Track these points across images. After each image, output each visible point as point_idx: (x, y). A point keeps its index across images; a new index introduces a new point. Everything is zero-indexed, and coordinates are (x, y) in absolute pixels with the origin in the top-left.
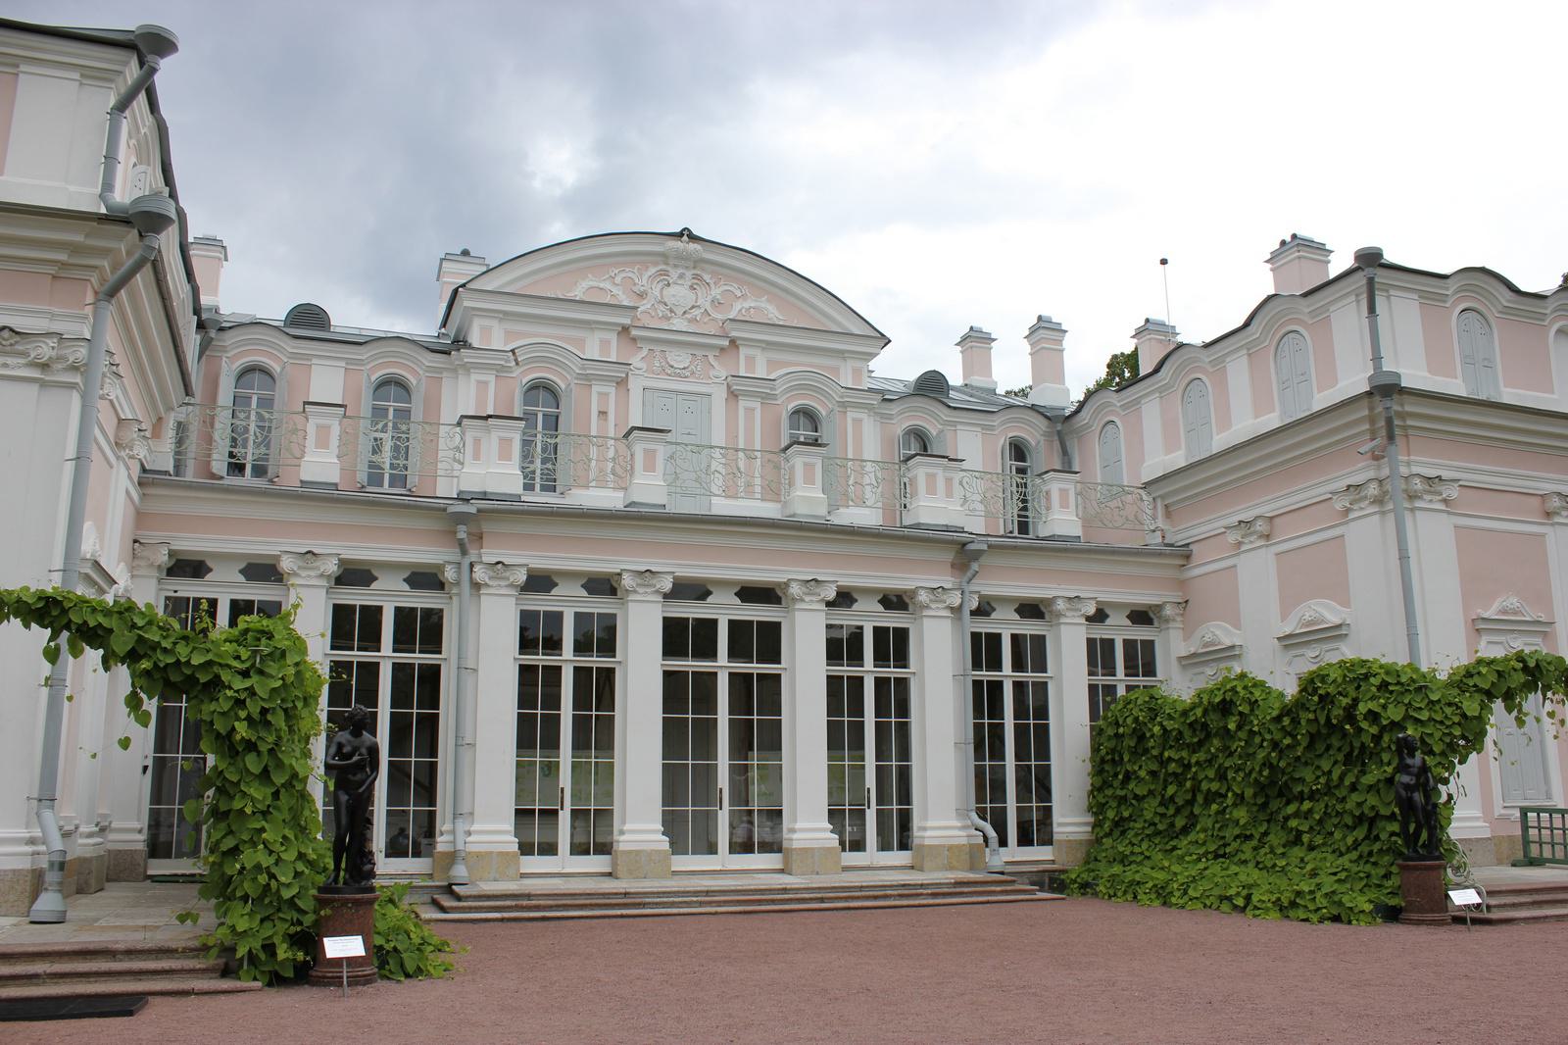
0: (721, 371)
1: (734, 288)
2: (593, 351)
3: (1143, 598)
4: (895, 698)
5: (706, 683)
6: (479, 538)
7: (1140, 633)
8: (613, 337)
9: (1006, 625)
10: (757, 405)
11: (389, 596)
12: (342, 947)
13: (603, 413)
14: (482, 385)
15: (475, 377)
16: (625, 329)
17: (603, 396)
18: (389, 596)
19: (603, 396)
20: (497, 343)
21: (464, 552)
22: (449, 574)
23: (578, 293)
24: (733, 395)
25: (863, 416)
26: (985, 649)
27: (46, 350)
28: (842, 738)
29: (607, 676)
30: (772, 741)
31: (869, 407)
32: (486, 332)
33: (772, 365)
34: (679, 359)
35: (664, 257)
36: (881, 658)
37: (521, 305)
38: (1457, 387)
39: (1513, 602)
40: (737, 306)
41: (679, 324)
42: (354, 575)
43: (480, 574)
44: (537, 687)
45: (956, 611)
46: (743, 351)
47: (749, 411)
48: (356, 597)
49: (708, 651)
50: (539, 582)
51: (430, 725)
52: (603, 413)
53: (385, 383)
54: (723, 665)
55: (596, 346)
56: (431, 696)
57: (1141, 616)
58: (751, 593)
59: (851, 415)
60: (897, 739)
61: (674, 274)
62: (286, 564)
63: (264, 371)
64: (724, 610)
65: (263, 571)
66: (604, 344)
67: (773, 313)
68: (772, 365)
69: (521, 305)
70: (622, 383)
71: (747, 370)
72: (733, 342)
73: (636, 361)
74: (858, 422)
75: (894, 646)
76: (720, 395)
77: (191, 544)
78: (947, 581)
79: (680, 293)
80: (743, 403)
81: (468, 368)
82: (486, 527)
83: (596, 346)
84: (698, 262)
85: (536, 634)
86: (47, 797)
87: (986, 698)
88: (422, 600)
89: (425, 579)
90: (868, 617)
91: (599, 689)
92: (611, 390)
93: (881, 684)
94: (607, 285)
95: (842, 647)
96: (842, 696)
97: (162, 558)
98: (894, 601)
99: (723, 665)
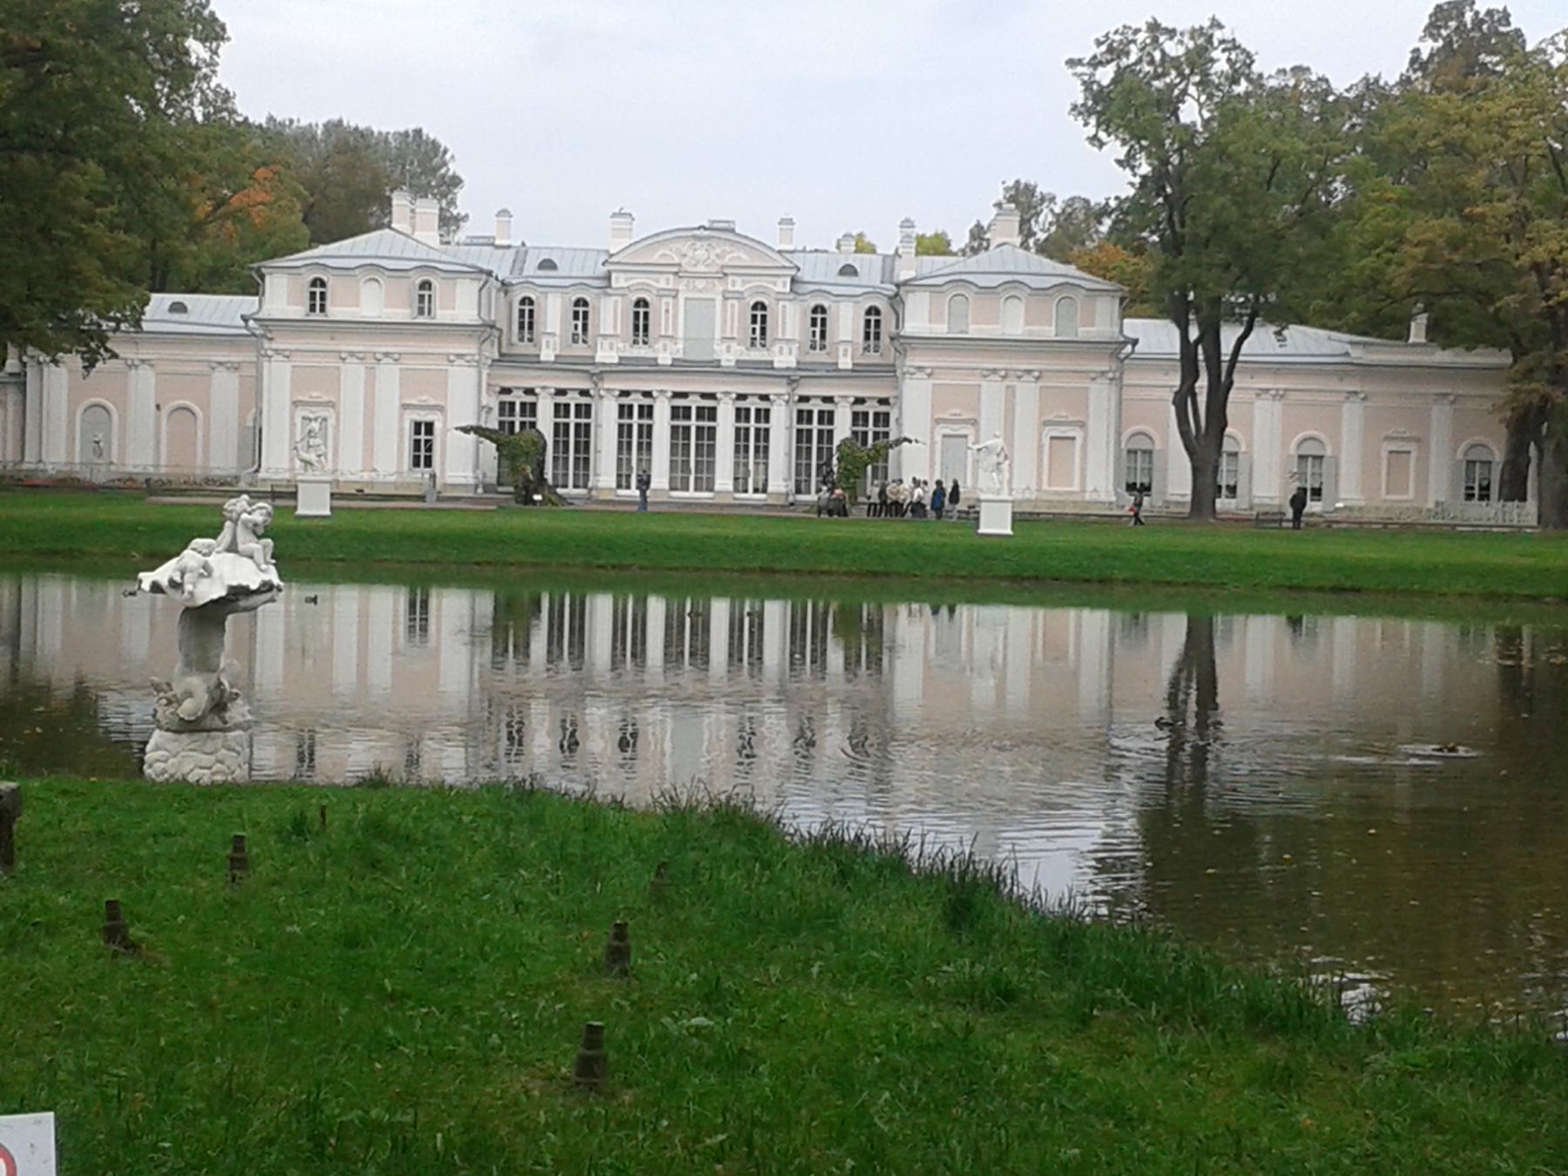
0: (720, 288)
1: (727, 248)
2: (662, 285)
3: (883, 395)
4: (763, 435)
5: (687, 429)
6: (602, 379)
7: (883, 409)
8: (671, 277)
9: (816, 407)
10: (735, 302)
11: (573, 399)
12: (537, 497)
13: (667, 311)
14: (616, 302)
15: (614, 298)
16: (676, 273)
17: (667, 304)
18: (573, 399)
19: (667, 304)
20: (623, 284)
21: (596, 385)
22: (592, 392)
23: (655, 259)
24: (726, 299)
25: (787, 303)
26: (805, 416)
27: (469, 358)
28: (740, 449)
29: (650, 427)
30: (712, 450)
31: (790, 300)
32: (617, 278)
33: (744, 282)
34: (700, 284)
35: (694, 237)
36: (758, 420)
37: (632, 268)
38: (941, 330)
39: (958, 411)
40: (728, 257)
41: (701, 268)
42: (561, 392)
43: (602, 393)
44: (624, 431)
45: (787, 402)
46: (730, 278)
47: (733, 306)
48: (562, 400)
49: (688, 417)
50: (625, 393)
51: (587, 444)
52: (667, 311)
53: (578, 302)
54: (693, 423)
55: (662, 283)
56: (587, 434)
57: (884, 401)
58: (704, 396)
59: (781, 303)
60: (763, 451)
61: (698, 244)
62: (537, 391)
63: (530, 299)
64: (694, 403)
65: (530, 392)
66: (668, 280)
67: (746, 258)
68: (744, 282)
69: (632, 268)
70: (675, 297)
71: (733, 285)
72: (726, 275)
73: (681, 287)
74: (784, 307)
75: (764, 415)
76: (719, 298)
77: (507, 384)
78: (783, 390)
79: (701, 253)
80: (730, 302)
81: (610, 295)
82: (605, 375)
83: (662, 283)
84: (709, 238)
85: (625, 411)
86: (476, 467)
87: (803, 437)
88: (584, 400)
89: (584, 393)
90: (753, 404)
91: (646, 432)
92: (670, 300)
93: (758, 430)
94: (668, 252)
95: (742, 414)
96: (741, 435)
97: (498, 389)
98: (765, 398)
99: (693, 423)
